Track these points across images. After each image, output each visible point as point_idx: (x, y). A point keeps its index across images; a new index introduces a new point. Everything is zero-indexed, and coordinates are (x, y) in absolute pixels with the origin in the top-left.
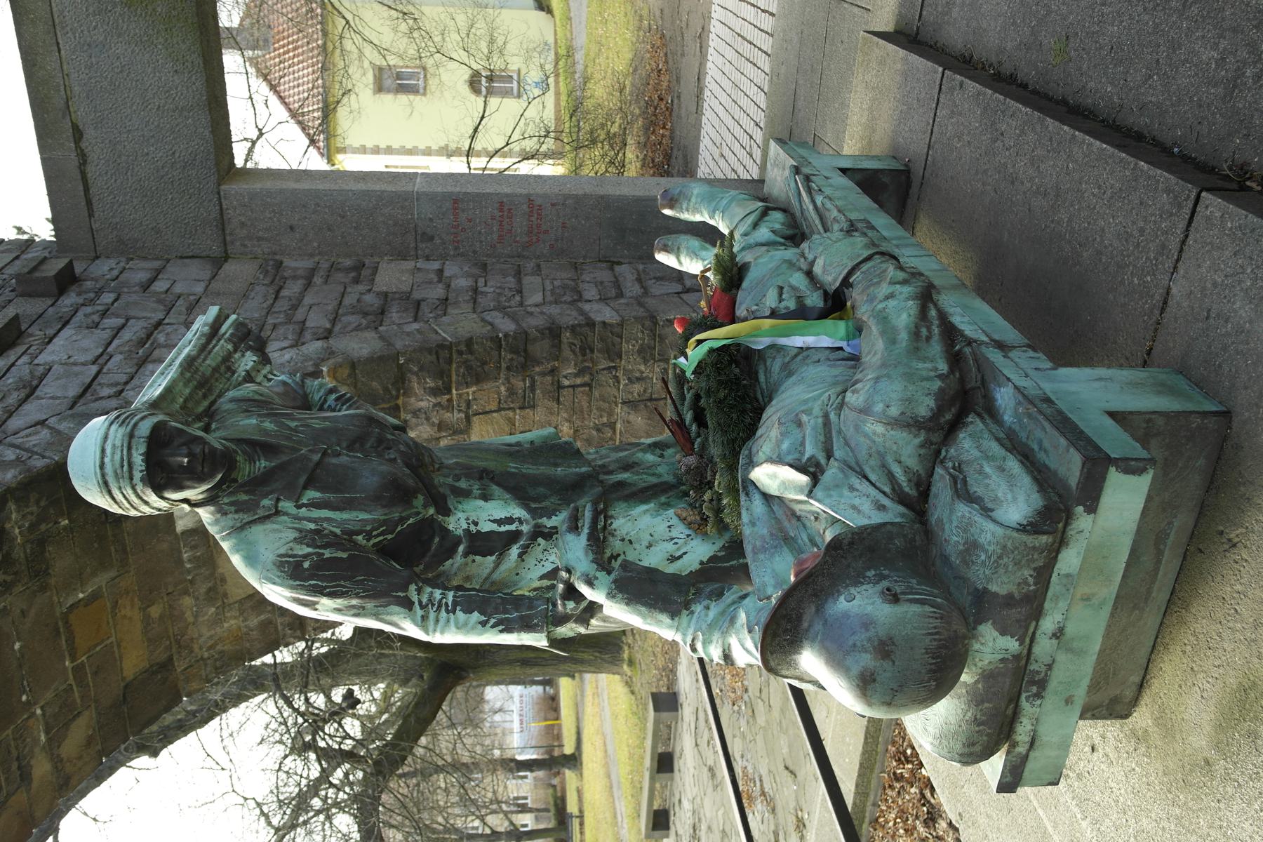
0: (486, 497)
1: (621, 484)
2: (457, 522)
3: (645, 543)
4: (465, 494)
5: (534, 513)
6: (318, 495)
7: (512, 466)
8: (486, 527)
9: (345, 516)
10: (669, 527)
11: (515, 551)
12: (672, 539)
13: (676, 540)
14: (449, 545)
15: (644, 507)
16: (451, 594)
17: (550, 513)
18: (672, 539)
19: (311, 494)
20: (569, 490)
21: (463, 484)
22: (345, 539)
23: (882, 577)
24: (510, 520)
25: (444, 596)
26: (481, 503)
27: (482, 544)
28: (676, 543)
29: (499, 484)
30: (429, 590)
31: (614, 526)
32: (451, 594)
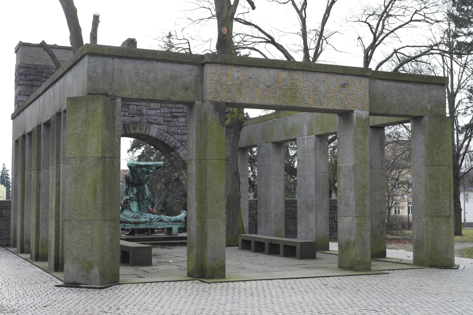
0: (137, 190)
1: (140, 203)
2: (134, 188)
5: (135, 194)
7: (141, 193)
8: (134, 190)
11: (132, 193)
14: (133, 187)
15: (137, 204)
17: (135, 196)
19: (132, 177)
20: (138, 197)
22: (129, 180)
27: (133, 190)
29: (138, 192)
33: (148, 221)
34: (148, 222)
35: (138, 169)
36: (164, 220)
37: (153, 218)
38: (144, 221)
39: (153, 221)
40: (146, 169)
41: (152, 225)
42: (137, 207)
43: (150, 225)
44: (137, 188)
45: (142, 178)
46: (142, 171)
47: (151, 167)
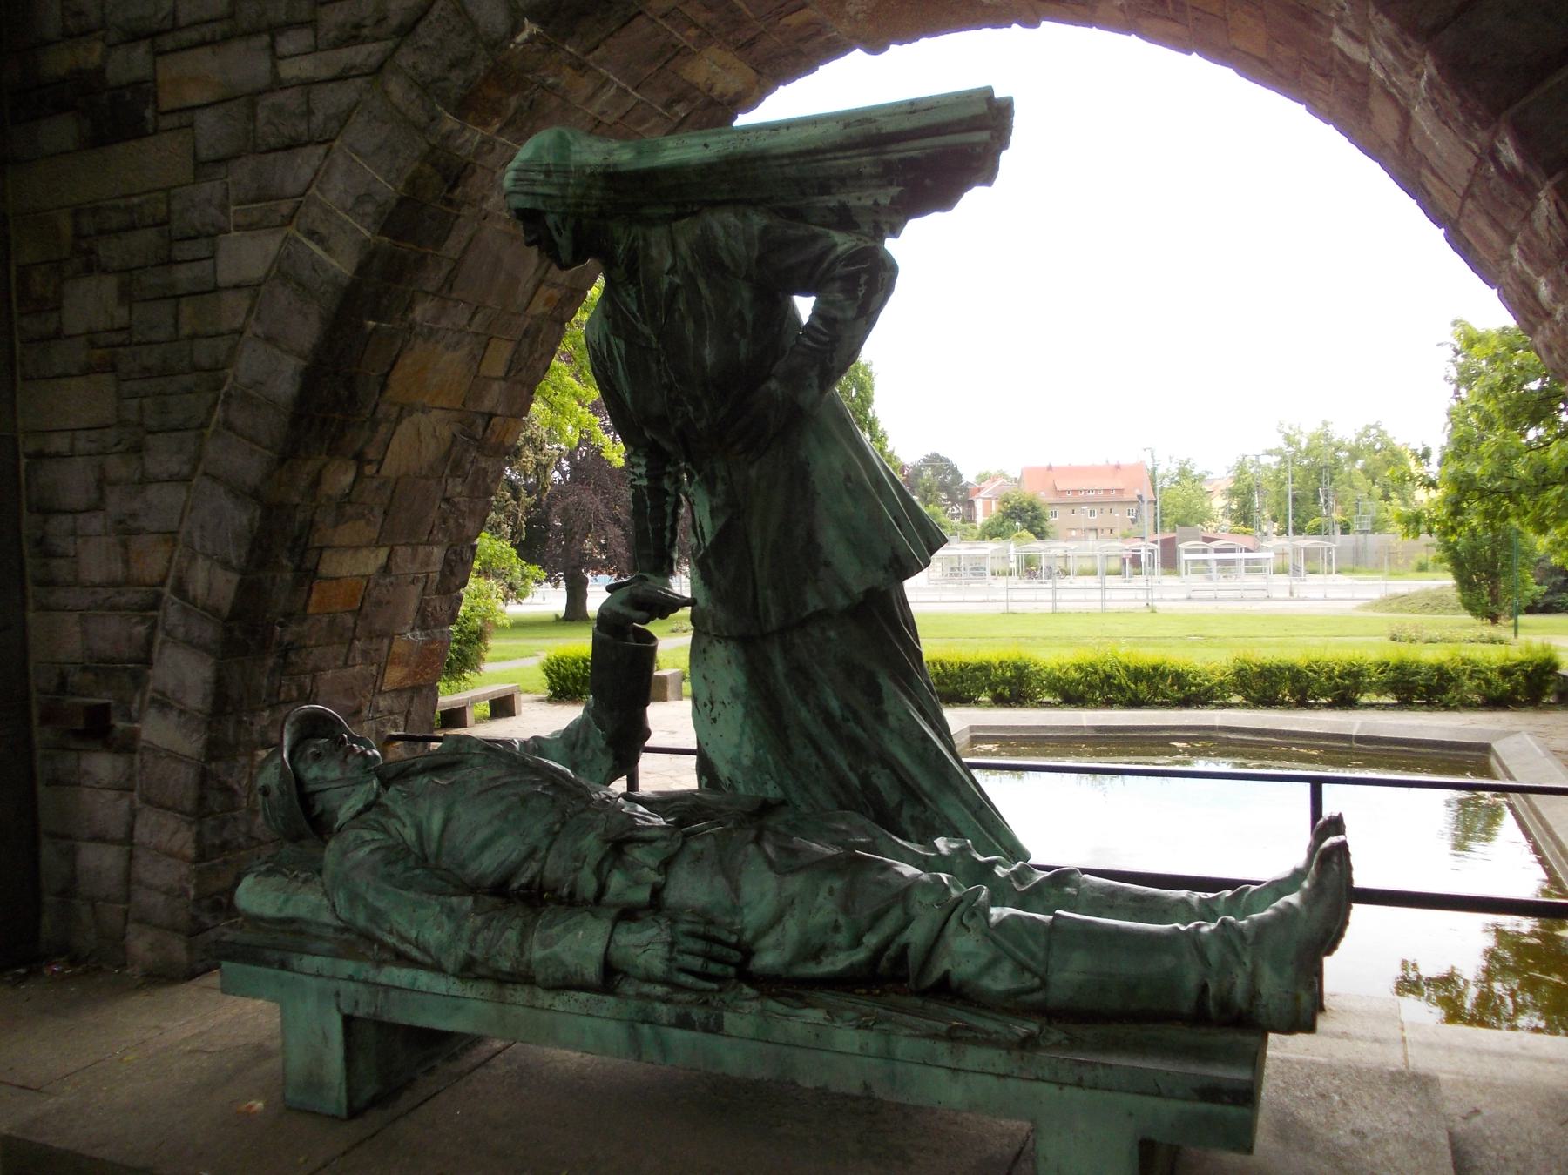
0: (713, 512)
3: (707, 676)
4: (711, 492)
6: (623, 352)
9: (623, 379)
10: (723, 703)
12: (712, 703)
13: (709, 706)
16: (644, 482)
18: (712, 703)
21: (720, 487)
23: (282, 793)
24: (704, 539)
25: (641, 476)
26: (708, 508)
28: (705, 705)
30: (643, 462)
31: (717, 645)
32: (644, 482)
33: (658, 967)
34: (649, 979)
35: (658, 234)
36: (942, 965)
37: (753, 917)
38: (592, 971)
39: (768, 959)
40: (758, 221)
41: (714, 1027)
42: (739, 711)
43: (684, 1022)
44: (709, 483)
45: (709, 354)
46: (709, 257)
47: (825, 188)
